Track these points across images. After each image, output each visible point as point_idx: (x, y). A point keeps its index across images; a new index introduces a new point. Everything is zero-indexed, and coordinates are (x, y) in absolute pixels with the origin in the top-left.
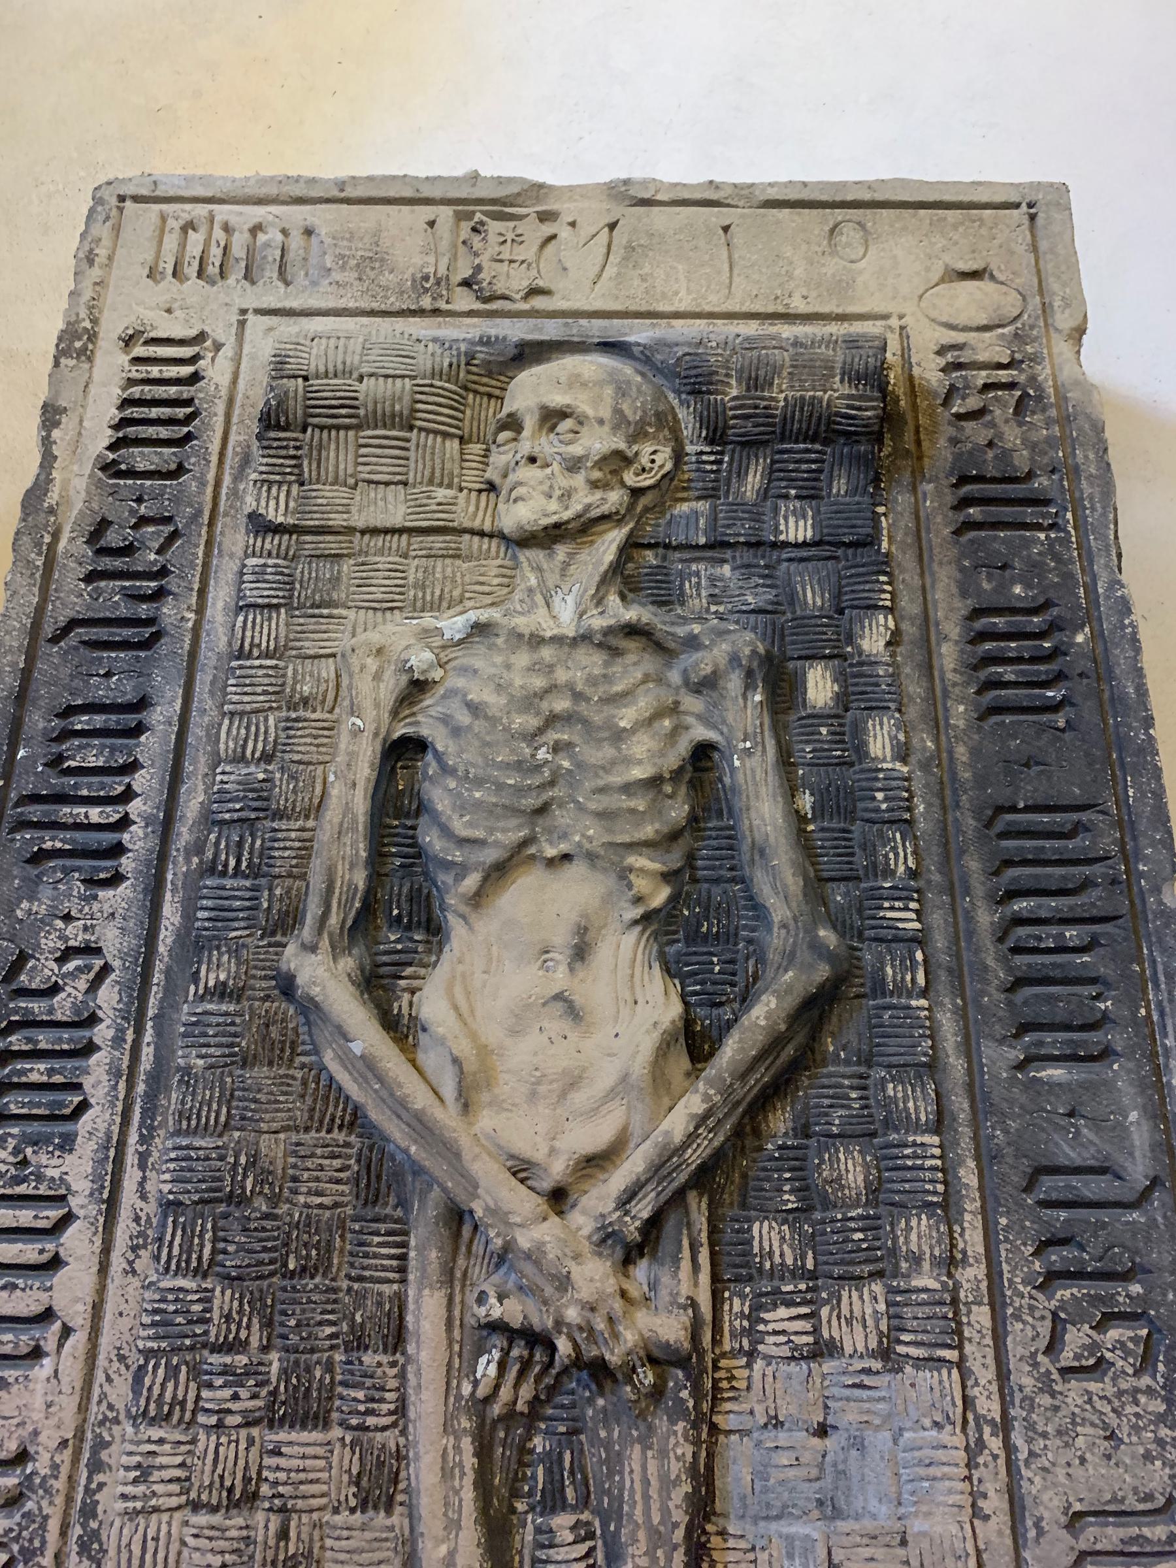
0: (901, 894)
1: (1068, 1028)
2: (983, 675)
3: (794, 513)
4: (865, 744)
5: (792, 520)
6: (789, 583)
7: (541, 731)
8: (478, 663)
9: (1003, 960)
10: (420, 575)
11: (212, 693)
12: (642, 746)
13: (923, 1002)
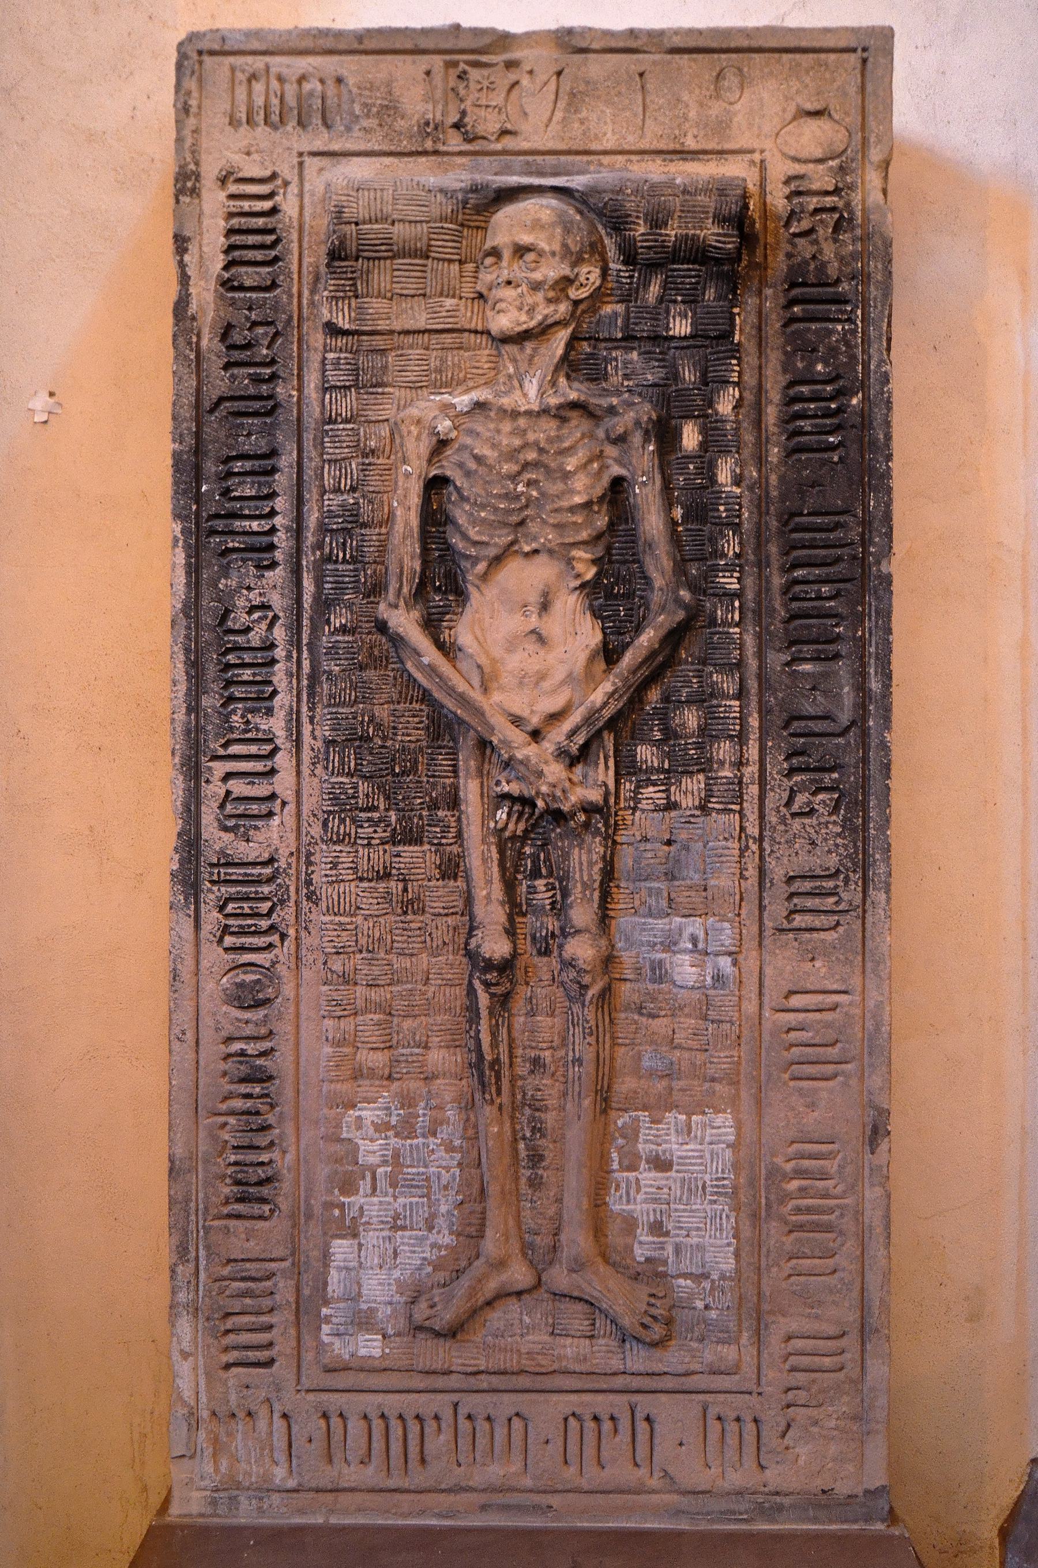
0: (729, 568)
1: (816, 642)
2: (791, 427)
3: (680, 314)
4: (716, 475)
5: (678, 319)
6: (674, 366)
7: (519, 473)
8: (480, 429)
9: (785, 605)
10: (438, 363)
11: (315, 446)
12: (580, 482)
13: (737, 630)
